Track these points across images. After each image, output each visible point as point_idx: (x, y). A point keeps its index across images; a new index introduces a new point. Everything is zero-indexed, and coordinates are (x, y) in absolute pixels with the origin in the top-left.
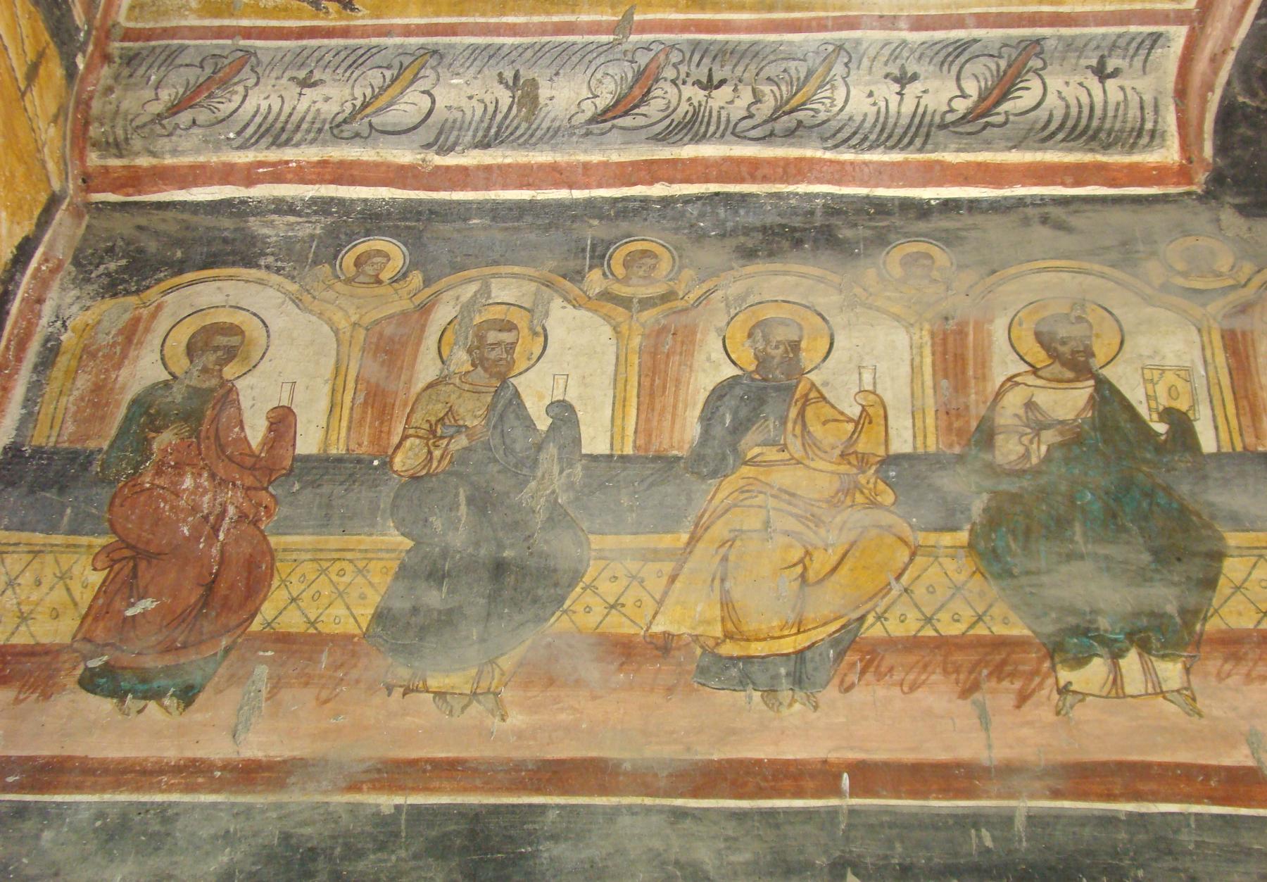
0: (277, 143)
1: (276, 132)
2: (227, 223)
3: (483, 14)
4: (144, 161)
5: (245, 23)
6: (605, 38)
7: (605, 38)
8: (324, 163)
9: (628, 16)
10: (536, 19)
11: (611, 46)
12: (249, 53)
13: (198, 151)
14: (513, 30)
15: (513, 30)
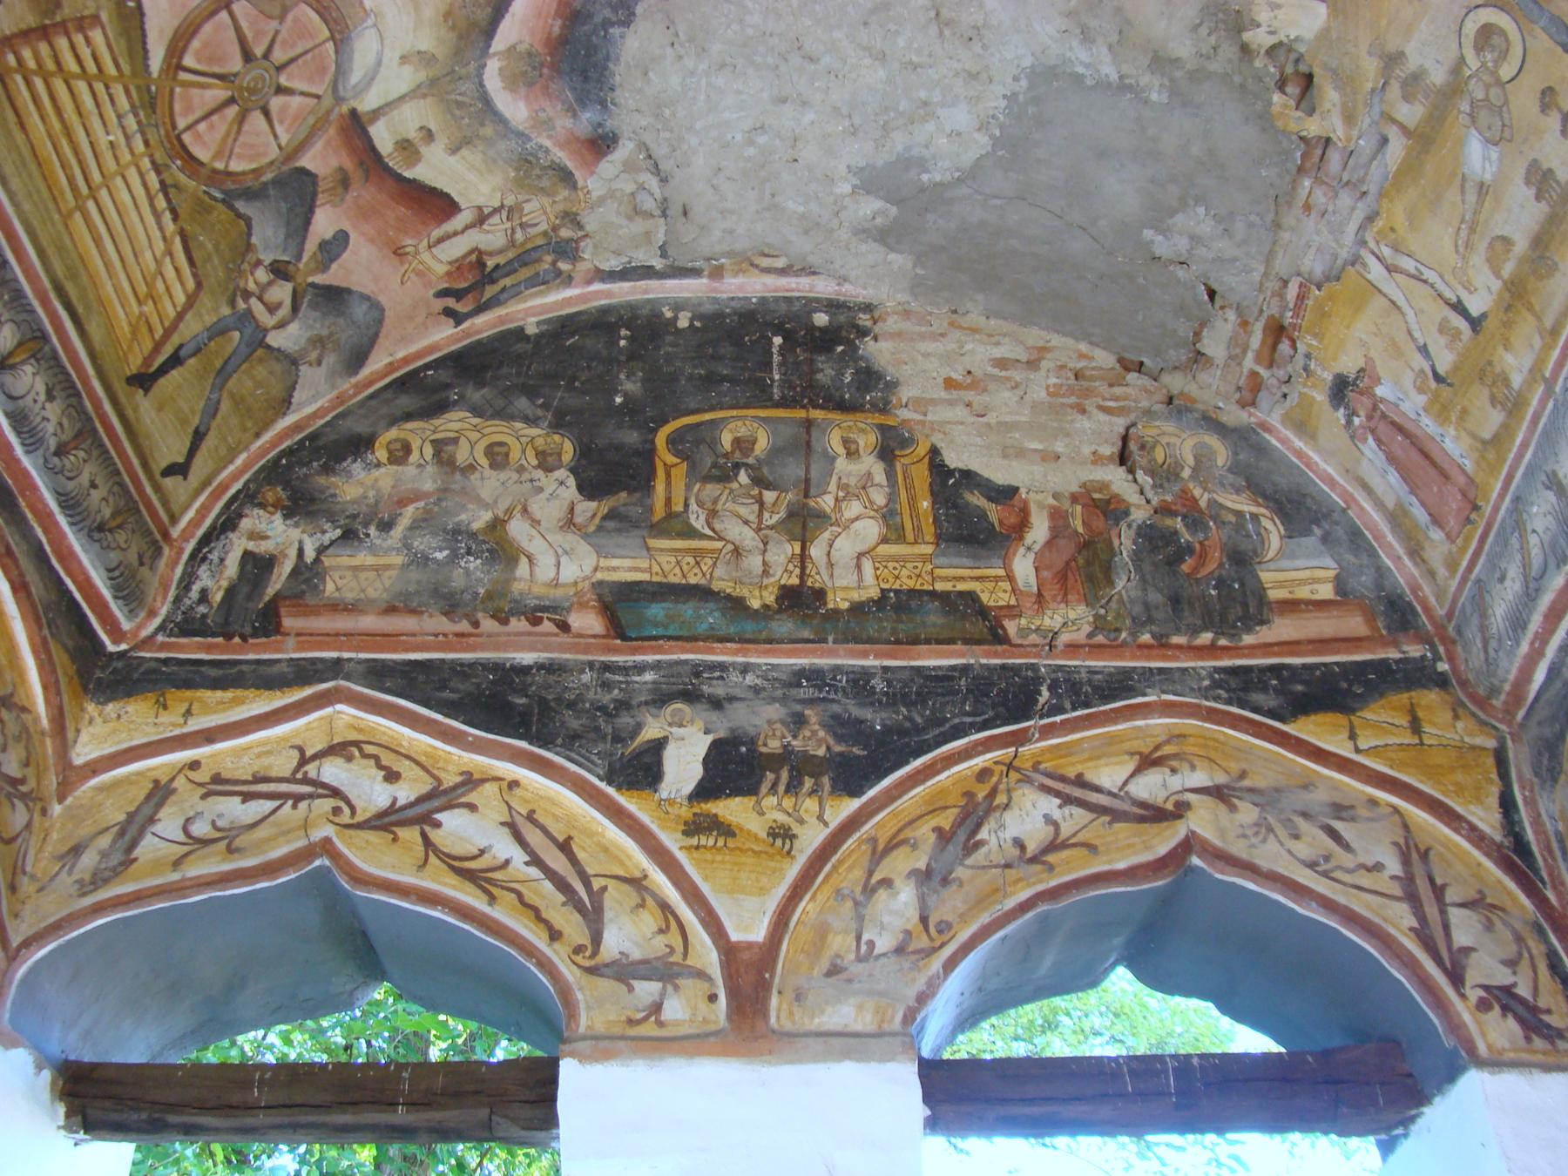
0: (1524, 627)
1: (1518, 623)
2: (1558, 684)
3: (1510, 450)
4: (1507, 687)
5: (1464, 564)
6: (1550, 405)
7: (1550, 405)
8: (1546, 617)
9: (1545, 380)
10: (1524, 427)
11: (1556, 400)
12: (1478, 581)
13: (1511, 663)
14: (1524, 446)
15: (1524, 446)
